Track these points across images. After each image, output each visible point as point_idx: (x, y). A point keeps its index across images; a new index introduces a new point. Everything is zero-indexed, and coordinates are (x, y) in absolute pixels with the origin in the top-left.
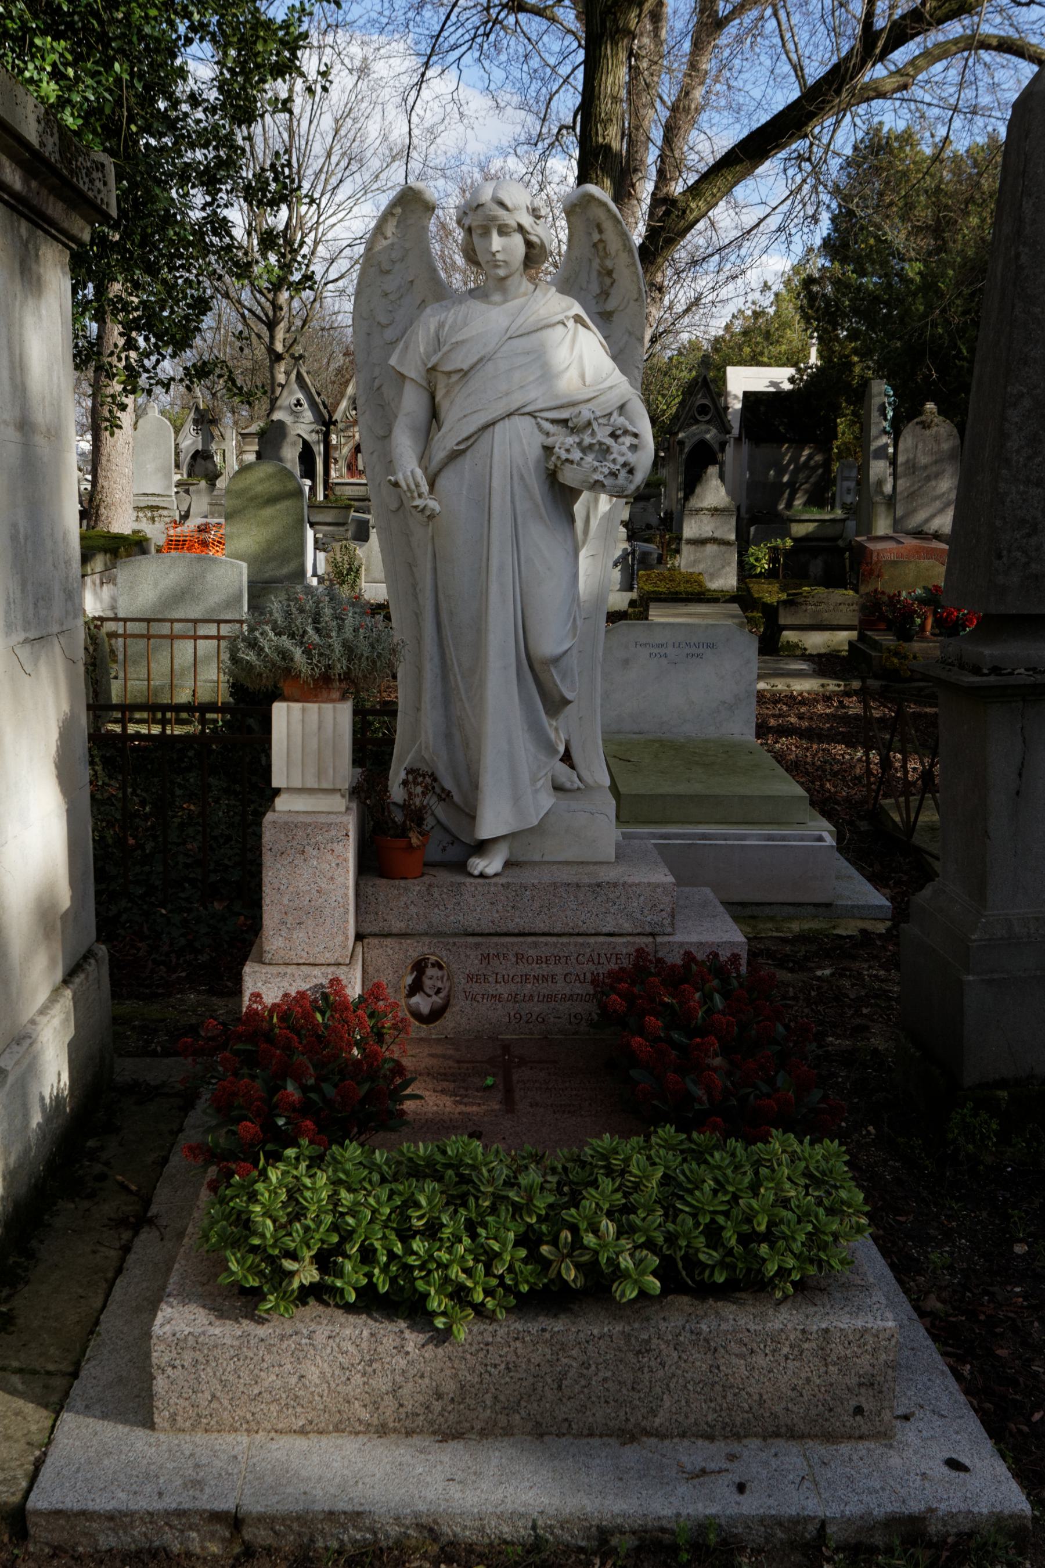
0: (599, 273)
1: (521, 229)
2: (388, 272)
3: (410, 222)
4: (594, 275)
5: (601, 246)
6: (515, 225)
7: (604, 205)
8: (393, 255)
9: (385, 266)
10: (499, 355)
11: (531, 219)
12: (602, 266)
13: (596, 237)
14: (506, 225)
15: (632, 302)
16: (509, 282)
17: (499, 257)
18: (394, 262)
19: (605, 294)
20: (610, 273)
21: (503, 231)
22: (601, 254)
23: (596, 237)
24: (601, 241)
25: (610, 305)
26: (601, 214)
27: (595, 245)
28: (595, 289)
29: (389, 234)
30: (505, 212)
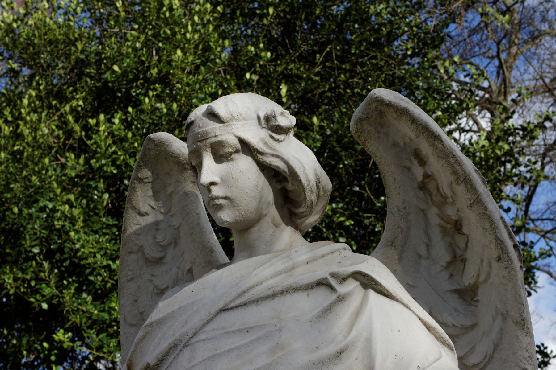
0: (444, 231)
1: (246, 147)
2: (159, 261)
3: (170, 189)
4: (436, 234)
5: (431, 186)
6: (236, 142)
7: (405, 112)
8: (160, 238)
9: (152, 252)
10: (202, 336)
11: (265, 133)
12: (443, 217)
13: (419, 172)
14: (220, 144)
15: (495, 264)
16: (254, 233)
17: (216, 191)
18: (164, 248)
19: (457, 260)
20: (458, 226)
21: (221, 155)
22: (437, 199)
23: (419, 172)
24: (426, 176)
25: (468, 279)
26: (406, 129)
27: (423, 187)
28: (442, 255)
29: (144, 208)
30: (217, 125)
